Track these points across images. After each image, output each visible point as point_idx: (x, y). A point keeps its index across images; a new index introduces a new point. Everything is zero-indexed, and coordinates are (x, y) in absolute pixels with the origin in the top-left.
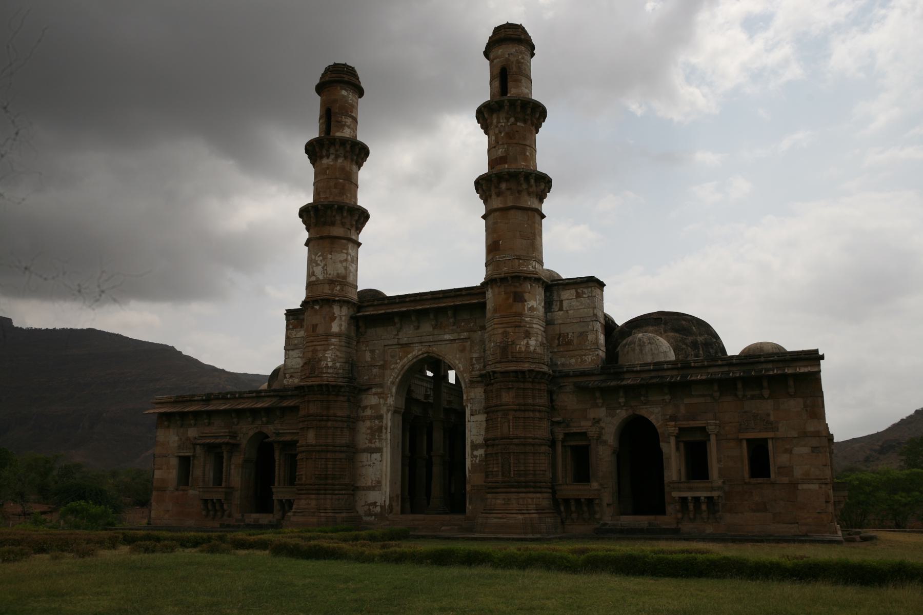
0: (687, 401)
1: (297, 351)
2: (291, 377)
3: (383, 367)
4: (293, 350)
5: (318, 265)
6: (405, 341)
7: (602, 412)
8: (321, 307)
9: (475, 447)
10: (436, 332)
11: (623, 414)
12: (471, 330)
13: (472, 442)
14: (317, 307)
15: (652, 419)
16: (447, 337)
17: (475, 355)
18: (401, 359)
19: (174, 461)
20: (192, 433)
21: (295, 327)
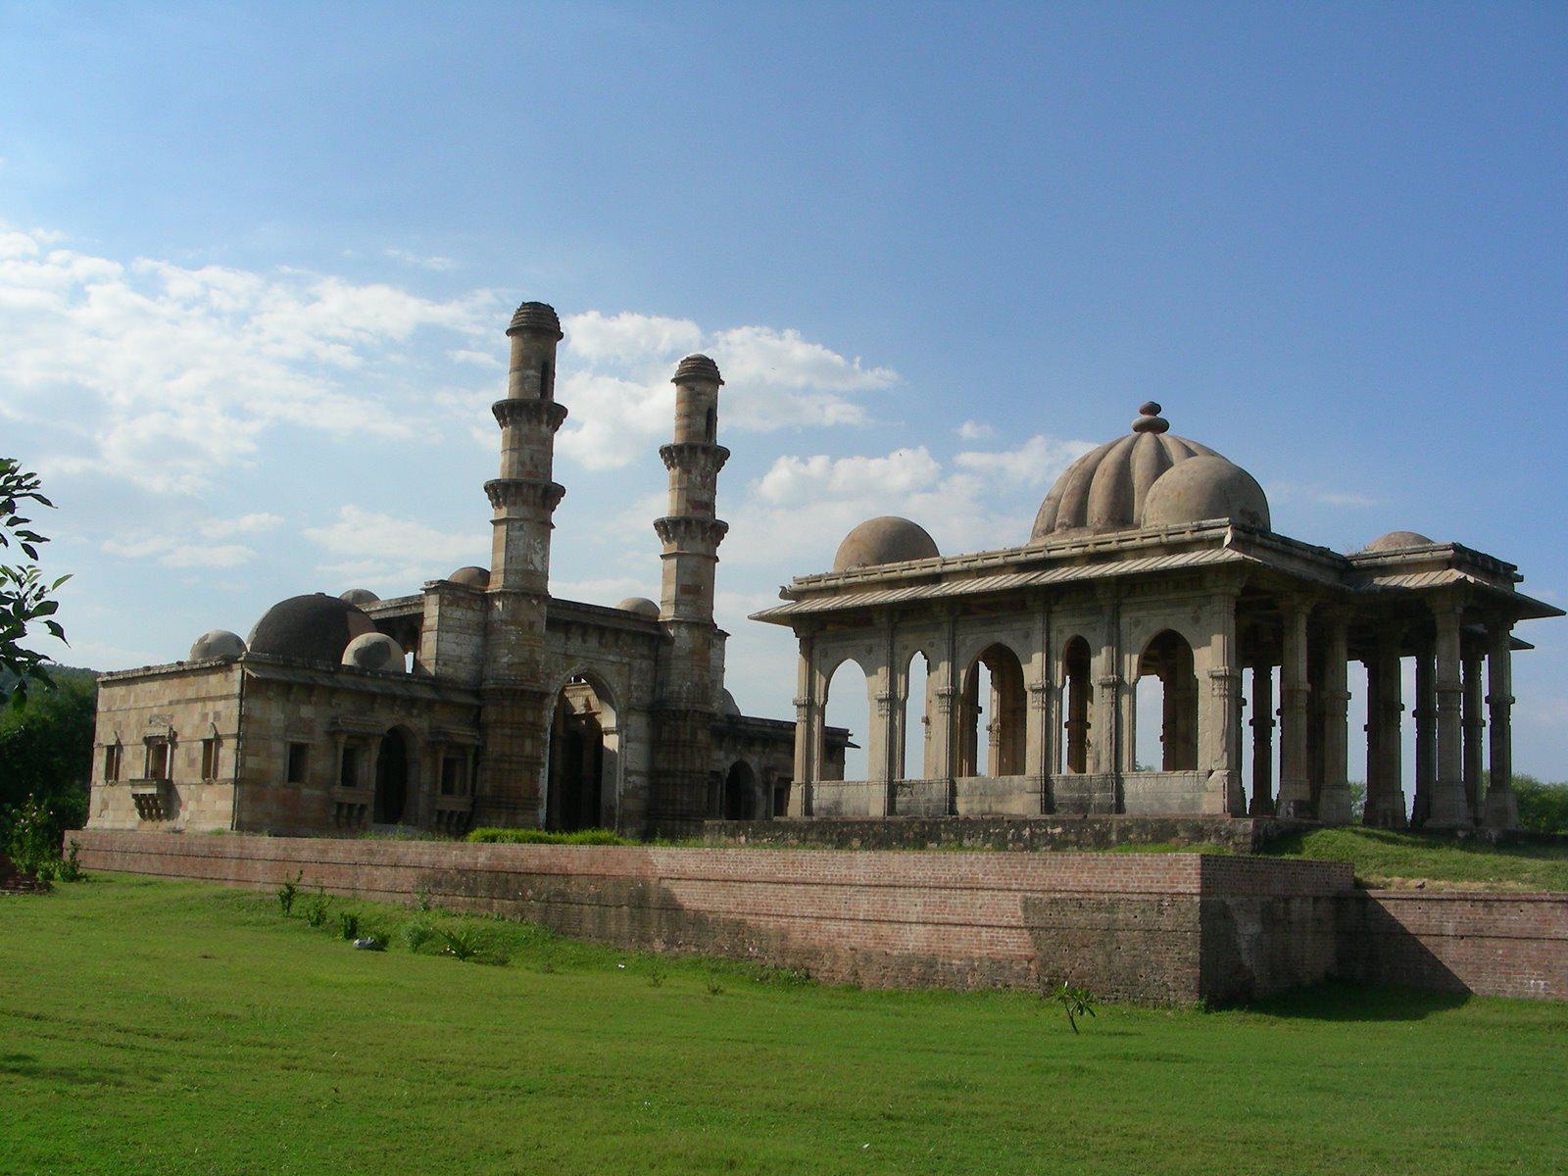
0: (775, 755)
1: (450, 635)
2: (445, 664)
3: (549, 676)
4: (447, 632)
5: (536, 553)
6: (571, 652)
7: (721, 755)
8: (539, 603)
9: (628, 772)
10: (603, 650)
11: (734, 758)
12: (632, 657)
13: (626, 769)
14: (535, 602)
15: (752, 765)
16: (611, 658)
17: (635, 683)
18: (565, 670)
19: (279, 747)
20: (306, 711)
21: (450, 604)
